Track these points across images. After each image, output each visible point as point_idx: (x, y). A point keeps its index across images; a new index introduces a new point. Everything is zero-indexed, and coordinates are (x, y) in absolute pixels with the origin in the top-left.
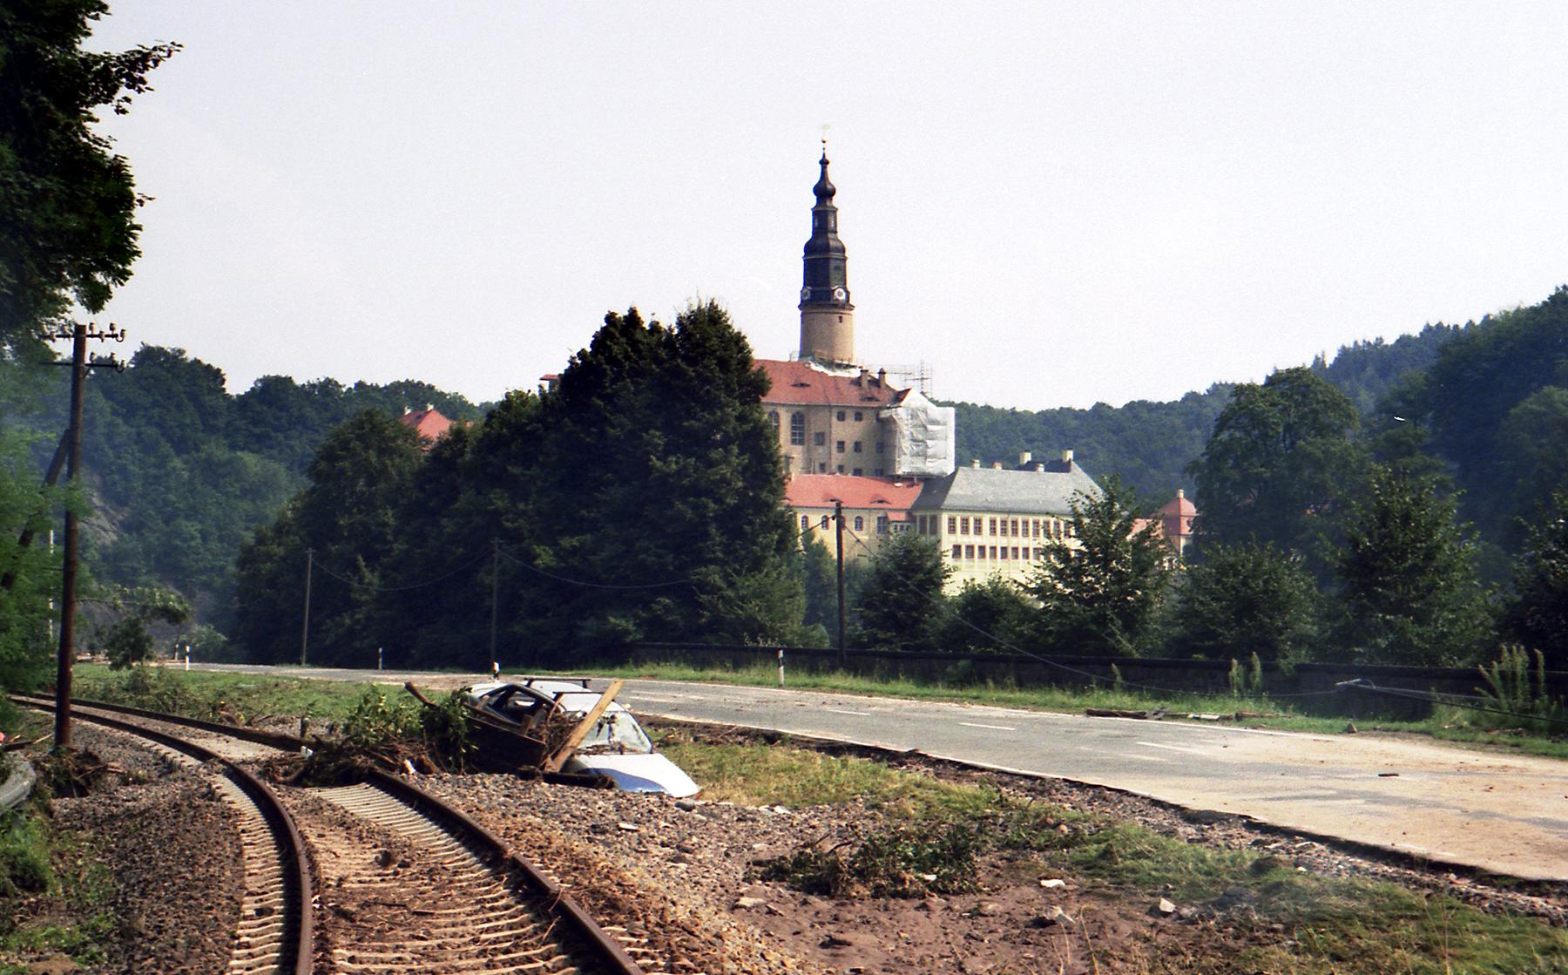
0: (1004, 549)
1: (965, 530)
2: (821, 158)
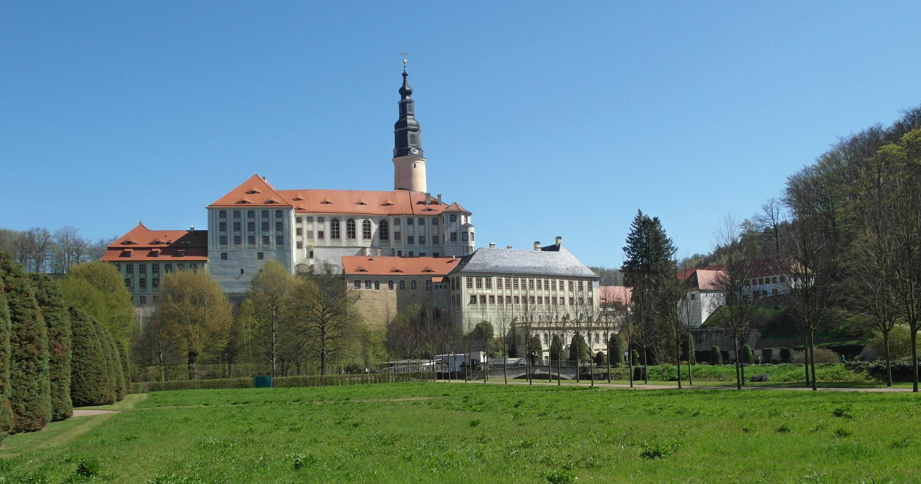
0: (509, 297)
1: (479, 286)
2: (403, 72)
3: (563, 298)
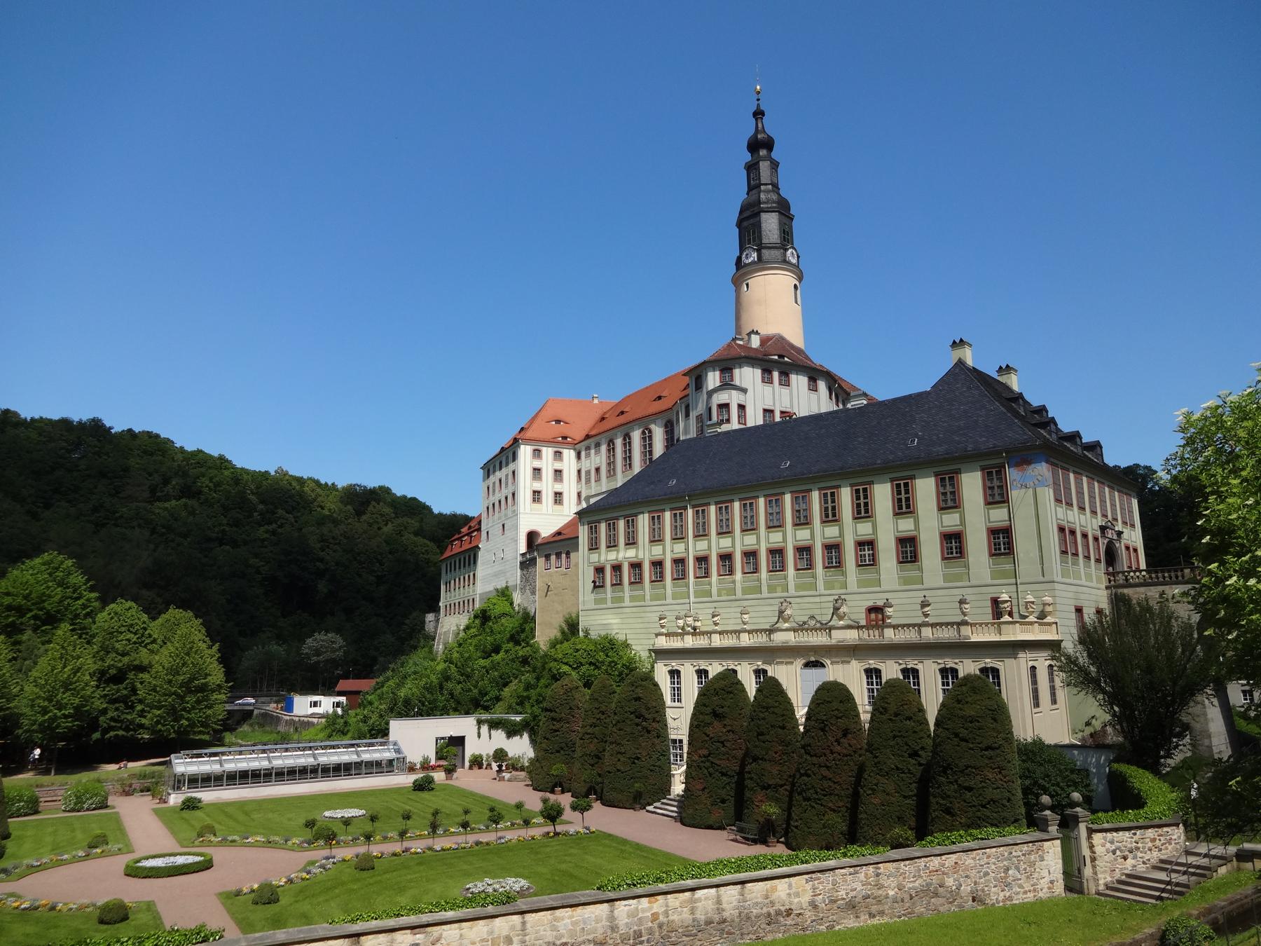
3: (867, 545)
